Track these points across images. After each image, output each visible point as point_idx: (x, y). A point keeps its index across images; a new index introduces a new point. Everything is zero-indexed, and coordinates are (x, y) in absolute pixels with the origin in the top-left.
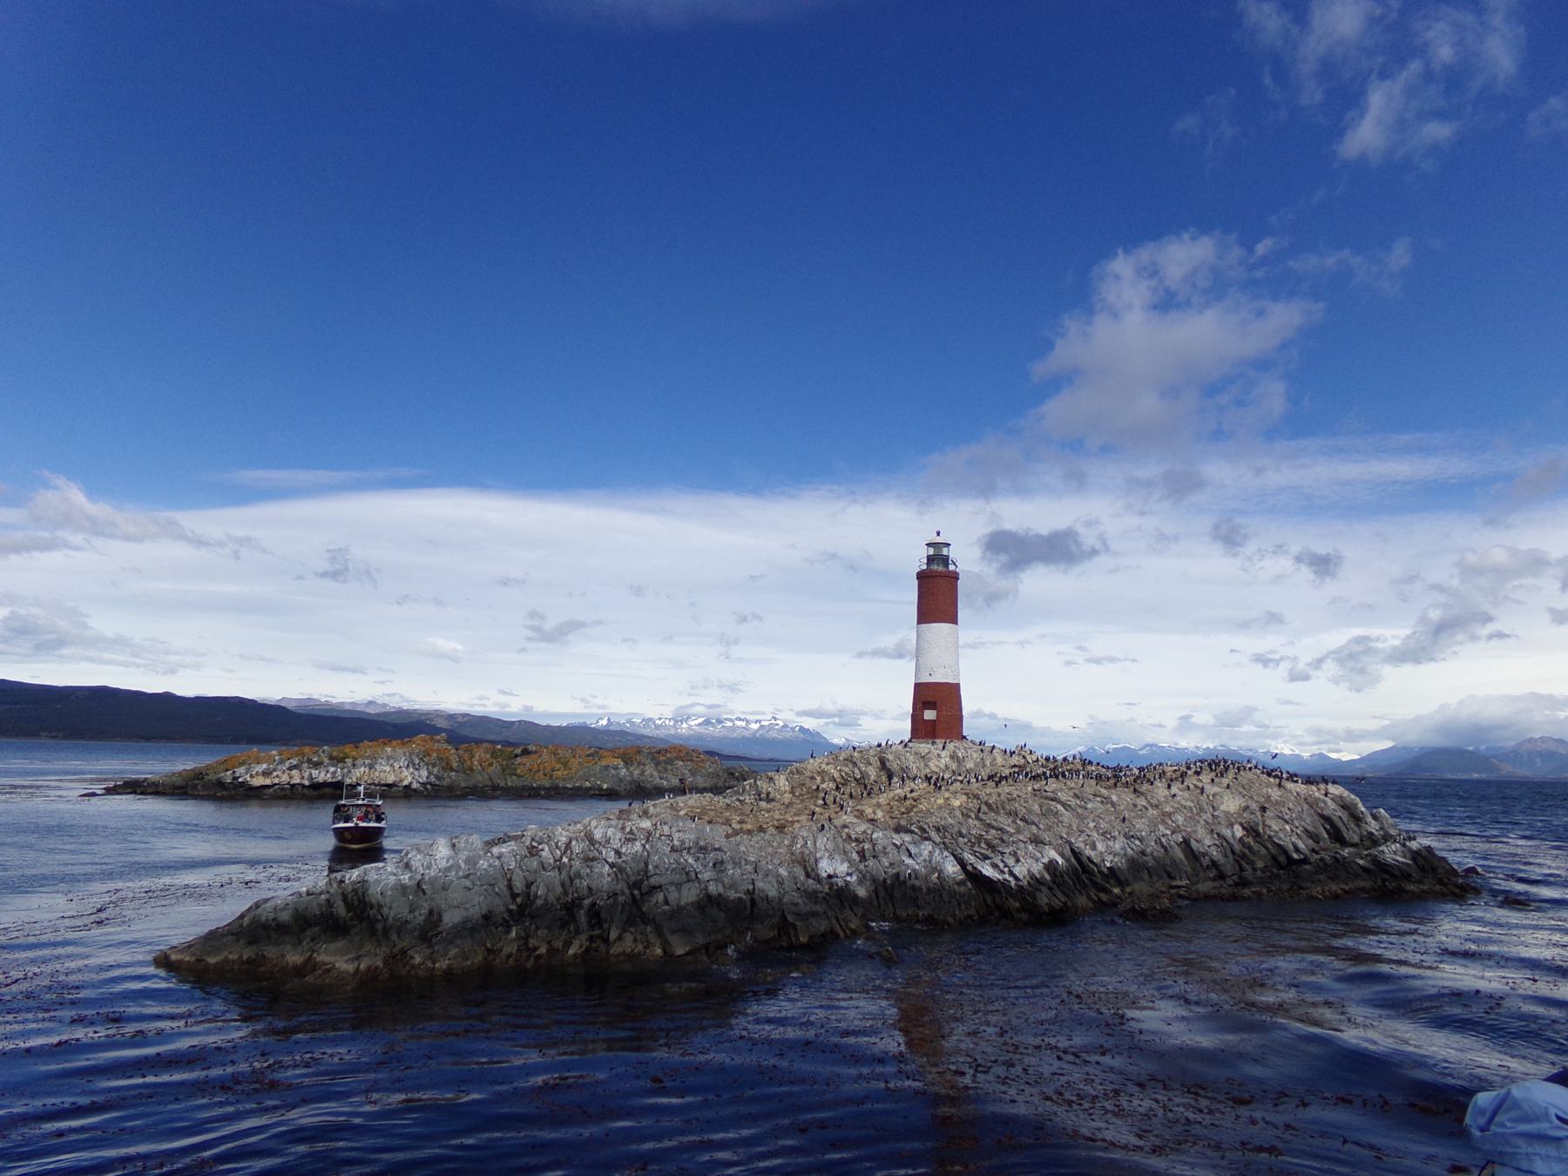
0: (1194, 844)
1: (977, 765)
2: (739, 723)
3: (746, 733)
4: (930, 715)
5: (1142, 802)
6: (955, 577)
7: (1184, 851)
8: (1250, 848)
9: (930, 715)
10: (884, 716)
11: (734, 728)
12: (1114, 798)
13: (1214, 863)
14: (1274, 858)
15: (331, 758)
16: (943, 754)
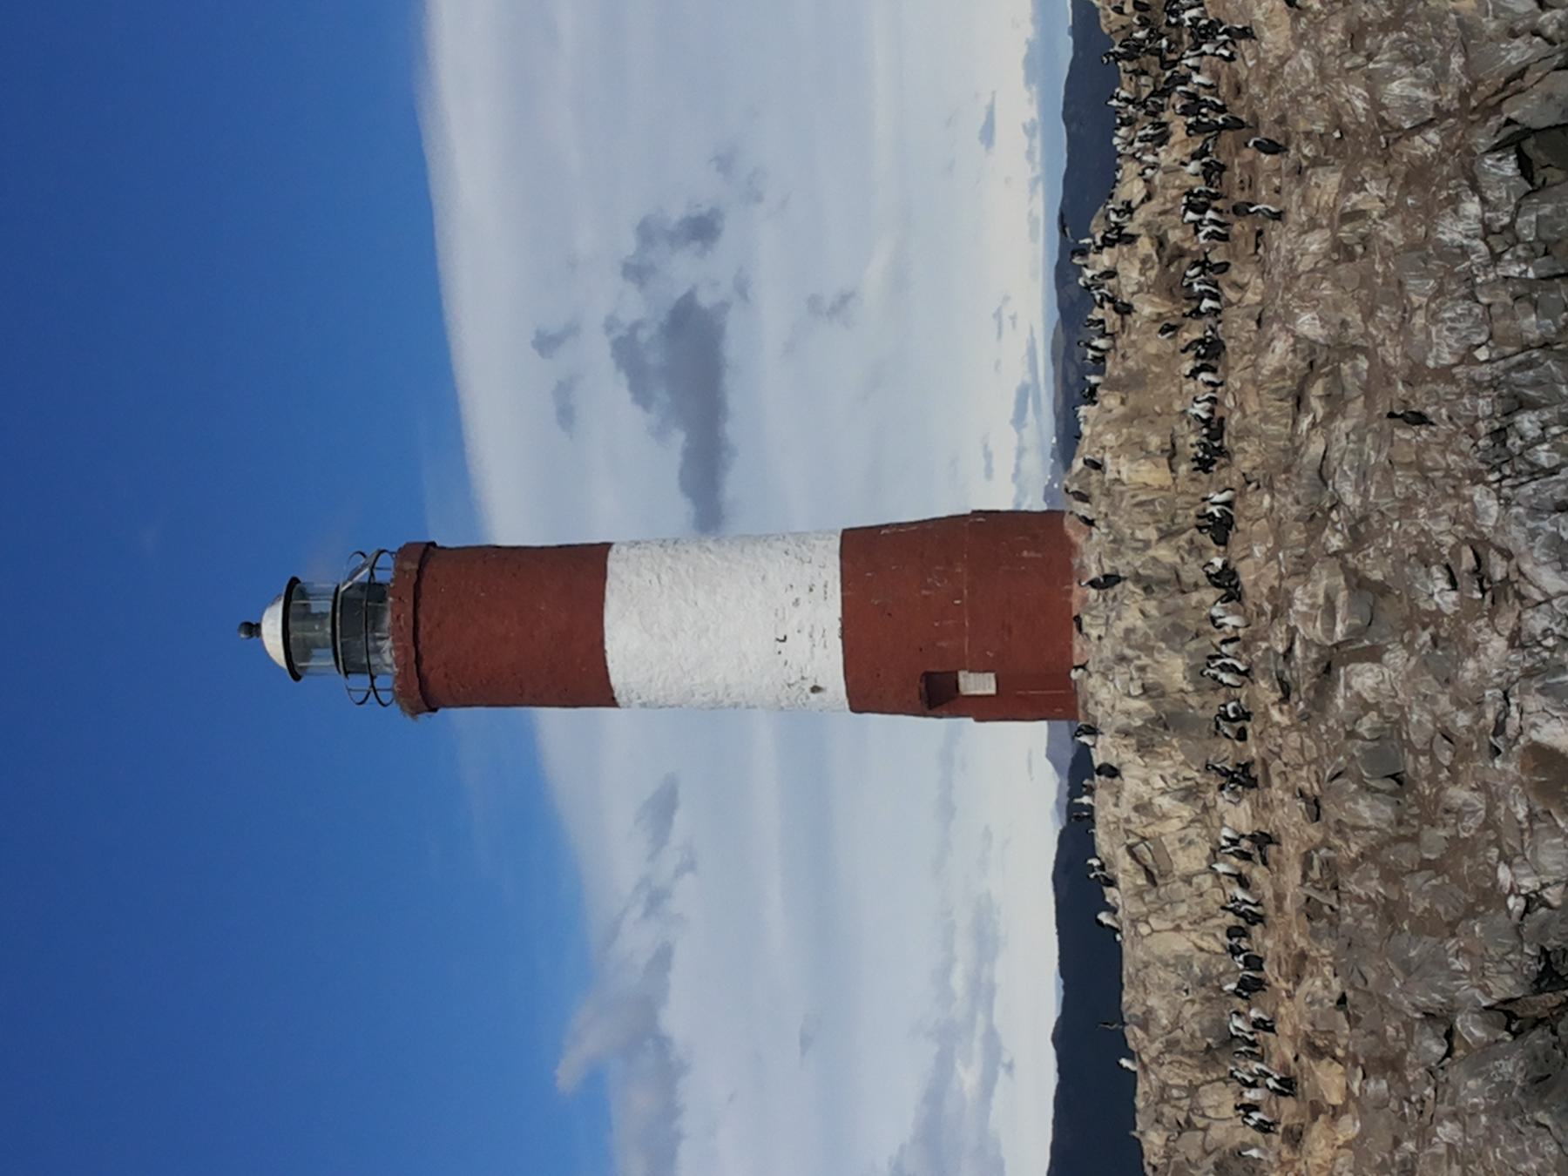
0: (1526, 110)
1: (1175, 634)
12: (1308, 324)
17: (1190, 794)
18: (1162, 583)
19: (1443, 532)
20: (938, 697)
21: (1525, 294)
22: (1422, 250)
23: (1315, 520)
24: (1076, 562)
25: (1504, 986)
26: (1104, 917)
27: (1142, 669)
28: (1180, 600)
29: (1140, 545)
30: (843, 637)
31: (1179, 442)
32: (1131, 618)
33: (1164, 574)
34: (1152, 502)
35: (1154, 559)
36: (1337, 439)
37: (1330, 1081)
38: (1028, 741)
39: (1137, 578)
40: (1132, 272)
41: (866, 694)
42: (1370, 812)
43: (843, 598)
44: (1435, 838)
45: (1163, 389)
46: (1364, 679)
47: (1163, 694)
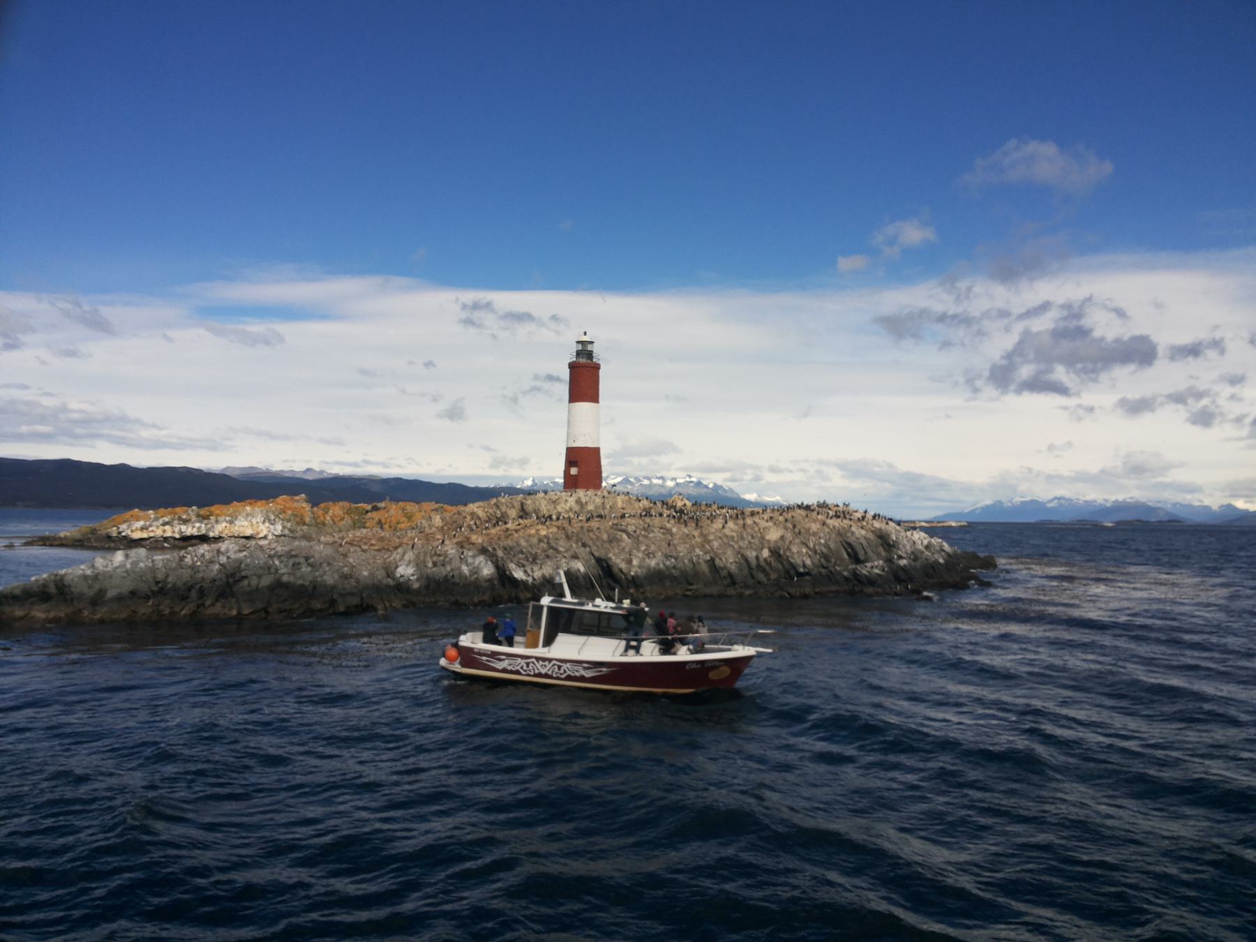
0: (717, 561)
1: (596, 507)
2: (655, 481)
3: (662, 491)
4: (574, 471)
5: (696, 533)
6: (597, 367)
7: (710, 567)
8: (770, 564)
9: (574, 471)
10: (553, 470)
11: (651, 486)
12: (674, 530)
13: (730, 575)
14: (787, 572)
15: (198, 516)
16: (570, 499)
17: (571, 509)
19: (653, 548)
20: (570, 462)
21: (691, 560)
22: (692, 548)
23: (644, 529)
25: (597, 554)
36: (657, 534)
37: (555, 530)
40: (645, 503)
41: (570, 450)
42: (605, 537)
44: (606, 545)
46: (625, 536)
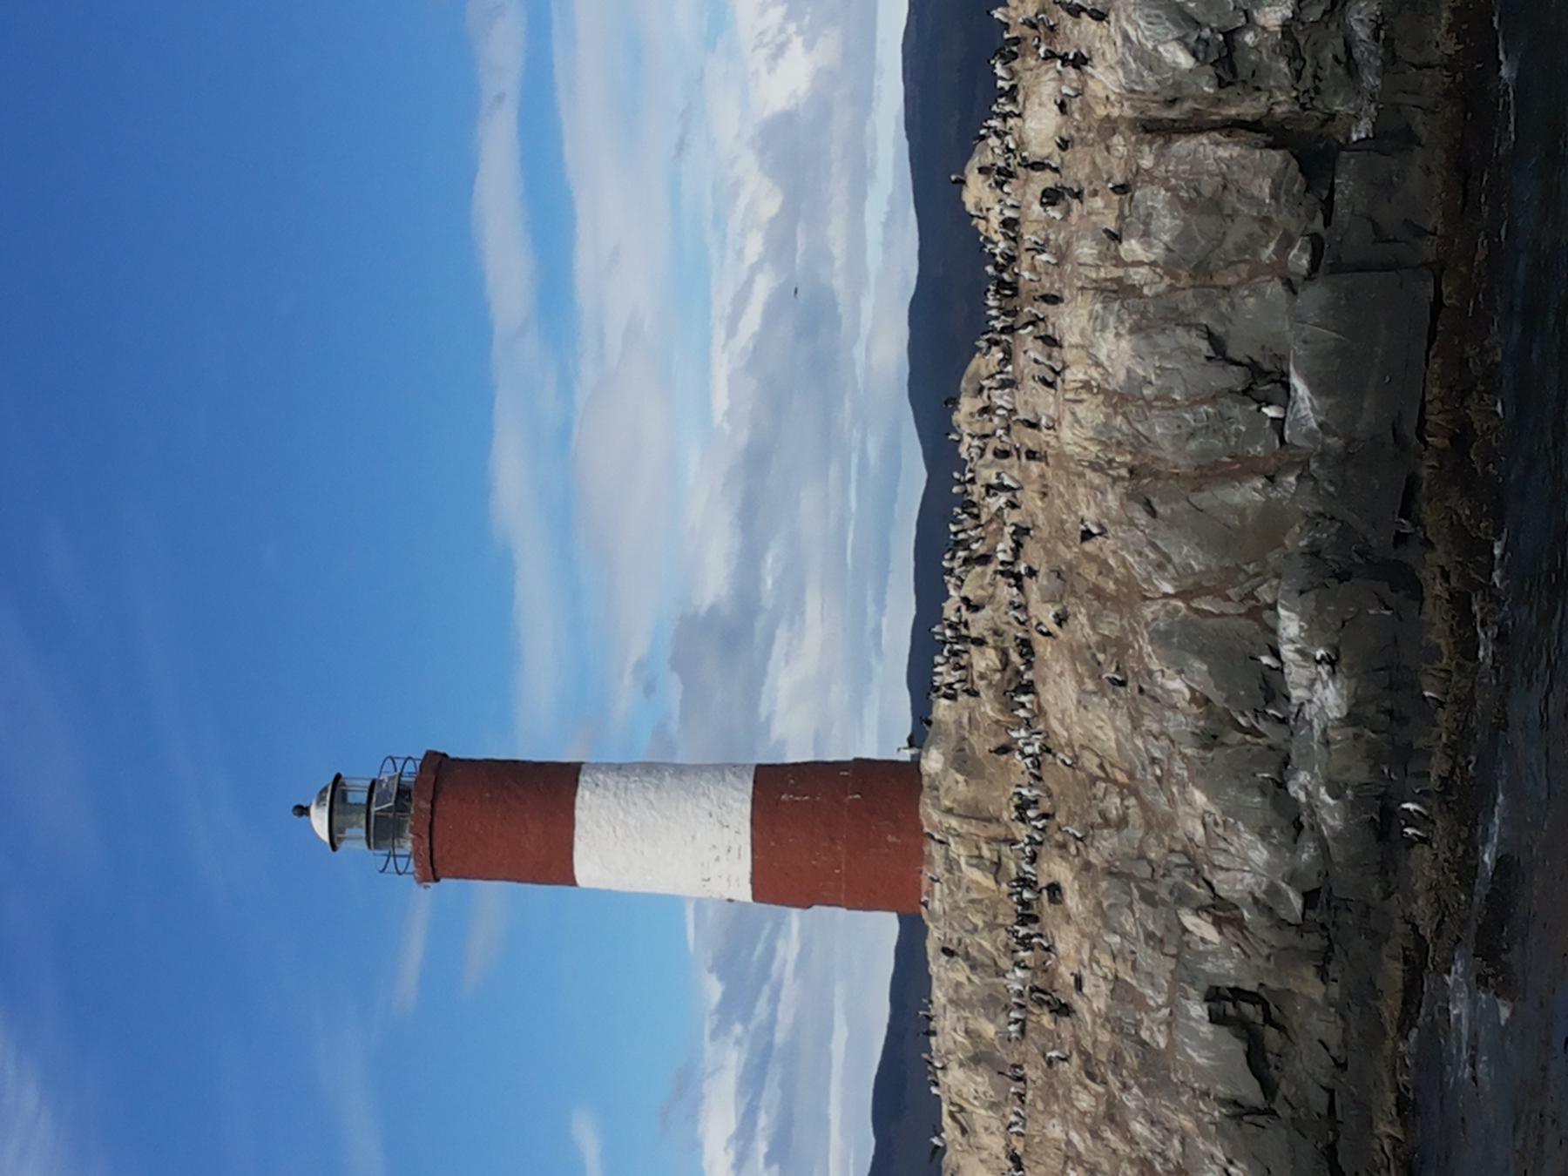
1: (993, 1003)
18: (983, 965)
24: (926, 849)
26: (934, 1090)
27: (966, 1018)
28: (997, 980)
29: (970, 927)
30: (753, 881)
31: (1004, 859)
32: (962, 978)
33: (988, 962)
34: (980, 901)
35: (980, 945)
38: (885, 927)
39: (967, 957)
43: (753, 860)
45: (996, 794)
47: (980, 1036)
